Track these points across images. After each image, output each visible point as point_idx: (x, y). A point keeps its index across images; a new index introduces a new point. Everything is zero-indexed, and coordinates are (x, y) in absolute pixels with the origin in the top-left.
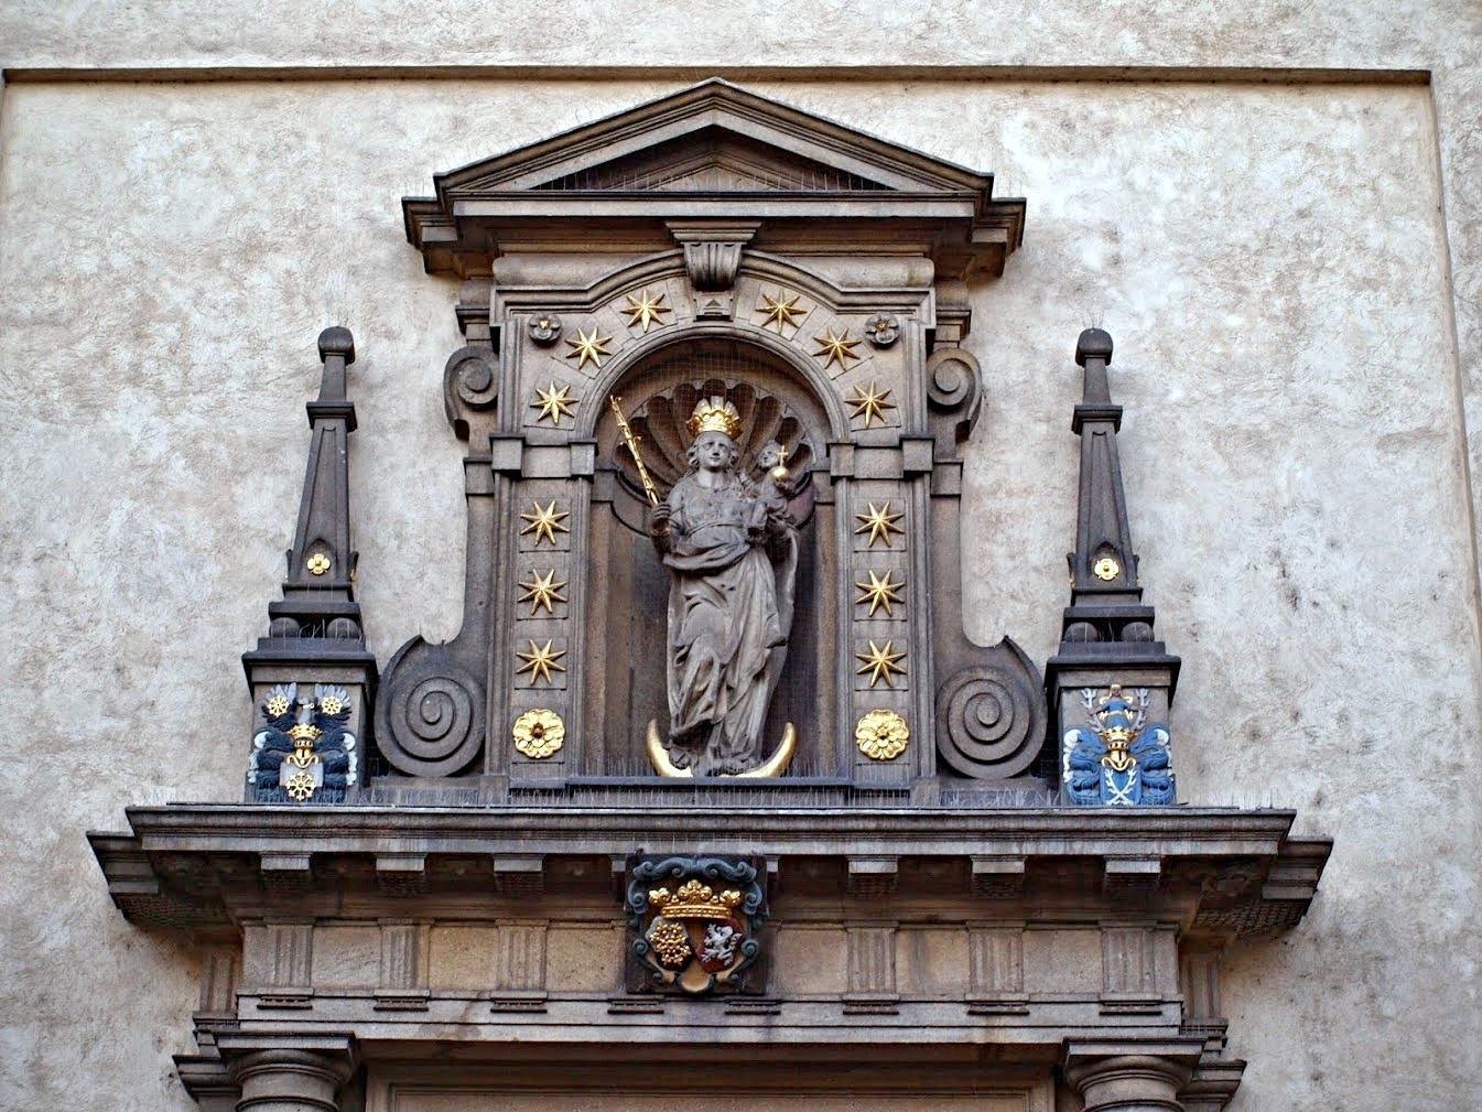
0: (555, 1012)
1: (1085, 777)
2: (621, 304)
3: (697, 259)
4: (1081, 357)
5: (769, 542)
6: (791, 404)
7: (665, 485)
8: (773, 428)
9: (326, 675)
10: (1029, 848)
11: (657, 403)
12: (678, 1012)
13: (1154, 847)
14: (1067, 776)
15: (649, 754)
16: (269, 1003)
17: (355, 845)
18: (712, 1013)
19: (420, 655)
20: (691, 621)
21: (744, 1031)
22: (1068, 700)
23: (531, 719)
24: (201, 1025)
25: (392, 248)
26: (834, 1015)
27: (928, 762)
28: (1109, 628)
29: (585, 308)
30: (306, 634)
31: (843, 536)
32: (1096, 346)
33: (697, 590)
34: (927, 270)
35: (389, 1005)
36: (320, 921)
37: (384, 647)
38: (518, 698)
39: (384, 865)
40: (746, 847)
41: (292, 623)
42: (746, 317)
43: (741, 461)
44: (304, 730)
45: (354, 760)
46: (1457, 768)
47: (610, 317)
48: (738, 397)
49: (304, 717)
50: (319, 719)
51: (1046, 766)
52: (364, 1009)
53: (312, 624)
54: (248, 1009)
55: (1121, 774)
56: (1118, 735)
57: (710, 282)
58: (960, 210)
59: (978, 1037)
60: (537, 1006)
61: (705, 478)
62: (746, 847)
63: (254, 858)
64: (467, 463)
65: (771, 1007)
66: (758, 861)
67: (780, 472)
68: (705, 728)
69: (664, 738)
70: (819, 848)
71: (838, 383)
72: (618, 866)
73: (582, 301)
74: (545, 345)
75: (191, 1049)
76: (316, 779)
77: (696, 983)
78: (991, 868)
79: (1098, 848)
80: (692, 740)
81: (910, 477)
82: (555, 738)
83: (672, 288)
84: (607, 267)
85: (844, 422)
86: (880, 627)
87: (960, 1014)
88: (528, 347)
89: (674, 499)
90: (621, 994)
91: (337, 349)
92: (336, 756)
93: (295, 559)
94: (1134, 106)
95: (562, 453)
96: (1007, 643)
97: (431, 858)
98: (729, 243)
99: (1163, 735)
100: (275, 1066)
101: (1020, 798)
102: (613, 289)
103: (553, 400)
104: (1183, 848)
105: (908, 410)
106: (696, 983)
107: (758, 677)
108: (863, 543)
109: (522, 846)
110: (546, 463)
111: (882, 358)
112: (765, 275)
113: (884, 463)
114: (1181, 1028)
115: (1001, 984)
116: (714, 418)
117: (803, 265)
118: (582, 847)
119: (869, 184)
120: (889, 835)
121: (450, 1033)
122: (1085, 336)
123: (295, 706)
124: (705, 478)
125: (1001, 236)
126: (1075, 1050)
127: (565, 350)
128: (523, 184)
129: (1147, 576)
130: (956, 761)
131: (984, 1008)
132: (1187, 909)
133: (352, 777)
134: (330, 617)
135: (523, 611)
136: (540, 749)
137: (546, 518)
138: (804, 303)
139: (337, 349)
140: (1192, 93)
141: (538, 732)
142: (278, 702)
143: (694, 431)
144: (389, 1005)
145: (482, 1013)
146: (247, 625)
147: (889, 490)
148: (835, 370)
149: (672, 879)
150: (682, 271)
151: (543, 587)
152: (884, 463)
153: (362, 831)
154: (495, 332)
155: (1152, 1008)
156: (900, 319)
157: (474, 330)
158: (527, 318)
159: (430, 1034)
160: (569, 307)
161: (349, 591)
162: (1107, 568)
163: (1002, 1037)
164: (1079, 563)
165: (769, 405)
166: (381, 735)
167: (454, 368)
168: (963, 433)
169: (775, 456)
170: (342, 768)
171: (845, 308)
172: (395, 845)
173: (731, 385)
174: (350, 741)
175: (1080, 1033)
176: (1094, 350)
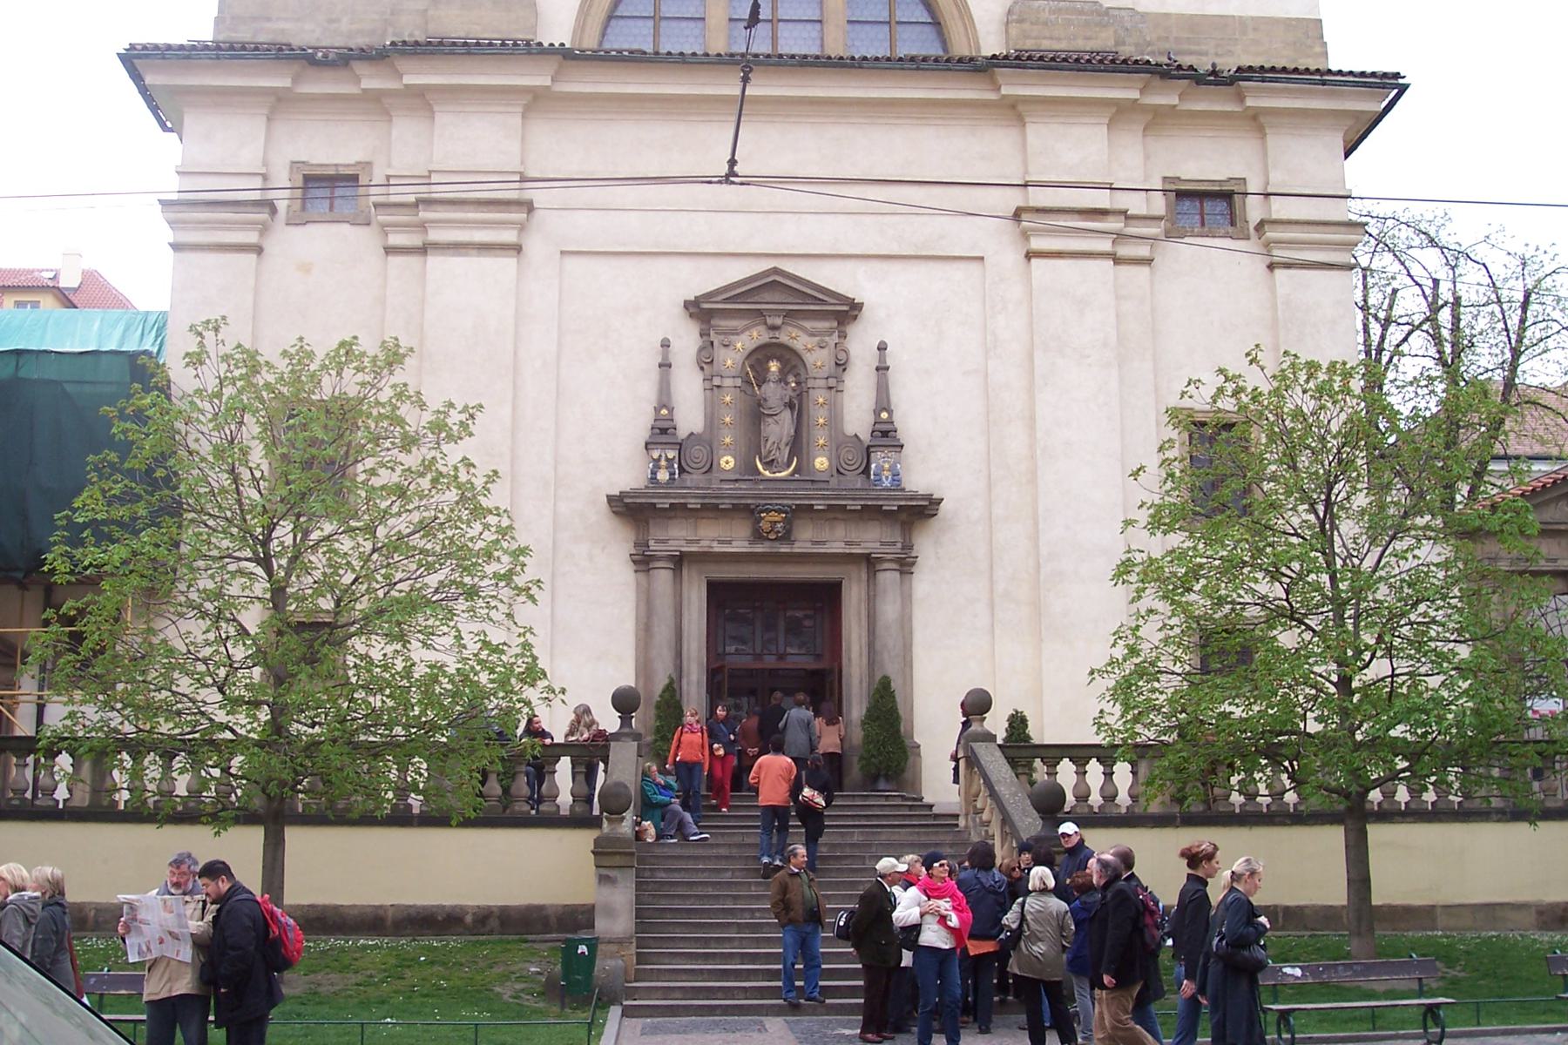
0: (734, 543)
1: (877, 478)
2: (747, 333)
3: (770, 321)
4: (879, 349)
5: (790, 405)
6: (794, 361)
7: (759, 386)
8: (789, 367)
9: (668, 446)
10: (863, 503)
11: (758, 359)
12: (767, 544)
13: (895, 503)
14: (872, 477)
15: (756, 466)
16: (658, 541)
17: (682, 501)
18: (777, 544)
19: (693, 437)
20: (769, 429)
21: (784, 549)
22: (872, 455)
23: (725, 458)
24: (636, 545)
25: (680, 309)
26: (809, 545)
27: (835, 472)
28: (885, 434)
29: (738, 334)
30: (661, 434)
31: (811, 405)
32: (883, 346)
33: (770, 420)
34: (835, 324)
35: (689, 542)
36: (670, 518)
37: (682, 433)
38: (721, 452)
39: (689, 506)
40: (785, 502)
41: (658, 431)
42: (783, 338)
43: (782, 380)
44: (663, 463)
45: (677, 471)
46: (980, 471)
47: (745, 337)
48: (779, 359)
49: (663, 459)
50: (667, 459)
51: (866, 471)
52: (683, 543)
53: (664, 431)
54: (651, 543)
55: (887, 478)
56: (887, 466)
57: (774, 328)
58: (845, 308)
59: (847, 551)
60: (729, 542)
61: (771, 384)
62: (785, 502)
63: (654, 504)
64: (704, 380)
65: (792, 542)
66: (790, 506)
67: (793, 385)
68: (773, 460)
69: (761, 461)
70: (807, 502)
71: (809, 358)
72: (752, 507)
73: (735, 332)
74: (725, 346)
75: (633, 552)
76: (667, 477)
77: (772, 536)
78: (853, 508)
79: (880, 503)
80: (769, 464)
81: (831, 388)
82: (732, 464)
83: (762, 328)
84: (745, 323)
85: (813, 372)
86: (821, 432)
87: (843, 545)
88: (722, 347)
89: (763, 387)
90: (752, 539)
91: (665, 344)
92: (672, 470)
93: (657, 410)
94: (896, 267)
95: (732, 380)
96: (856, 435)
97: (702, 504)
98: (779, 316)
99: (899, 466)
100: (659, 559)
101: (859, 482)
102: (747, 328)
103: (729, 362)
104: (903, 503)
105: (829, 367)
106: (772, 536)
107: (787, 445)
108: (817, 407)
109: (727, 501)
110: (728, 382)
111: (822, 350)
112: (790, 325)
113: (822, 383)
114: (902, 549)
115: (853, 536)
116: (774, 366)
117: (801, 323)
118: (743, 502)
119: (820, 300)
120: (823, 499)
121: (706, 550)
122: (880, 343)
123: (660, 456)
124: (771, 384)
125: (856, 313)
126: (873, 555)
127: (732, 347)
128: (720, 298)
129: (895, 418)
130: (842, 470)
131: (847, 543)
132: (904, 516)
133: (677, 476)
134: (668, 429)
135: (722, 426)
136: (728, 467)
137: (728, 399)
138: (800, 333)
139: (665, 344)
140: (913, 261)
141: (727, 463)
142: (656, 454)
143: (768, 370)
144: (689, 542)
145: (715, 544)
146: (643, 434)
147: (824, 391)
148: (809, 354)
149: (768, 511)
150: (766, 323)
151: (728, 419)
152: (822, 383)
153: (683, 497)
154: (712, 343)
155: (894, 543)
156: (827, 339)
157: (705, 338)
158: (722, 337)
159: (701, 550)
160: (733, 334)
161: (672, 420)
162: (884, 415)
163: (853, 551)
164: (877, 413)
165: (788, 361)
166: (682, 461)
167: (701, 350)
168: (844, 370)
169: (791, 378)
170: (674, 474)
171: (812, 335)
172: (693, 501)
173: (778, 354)
174: (676, 466)
175: (875, 551)
176: (882, 348)
